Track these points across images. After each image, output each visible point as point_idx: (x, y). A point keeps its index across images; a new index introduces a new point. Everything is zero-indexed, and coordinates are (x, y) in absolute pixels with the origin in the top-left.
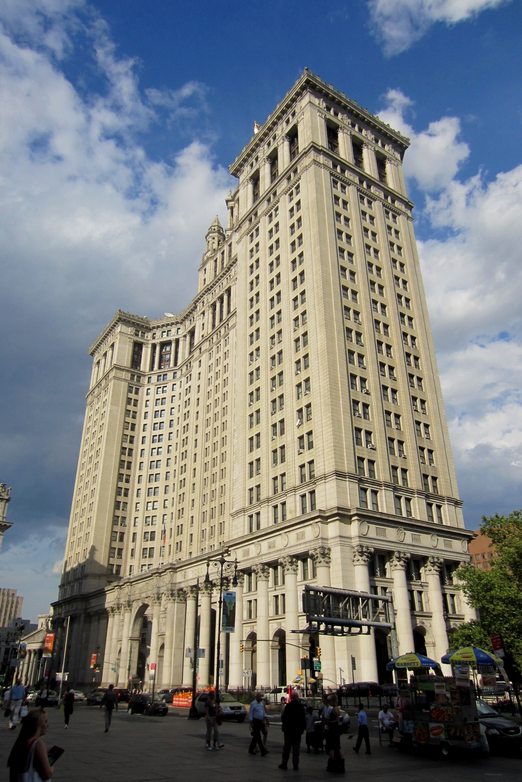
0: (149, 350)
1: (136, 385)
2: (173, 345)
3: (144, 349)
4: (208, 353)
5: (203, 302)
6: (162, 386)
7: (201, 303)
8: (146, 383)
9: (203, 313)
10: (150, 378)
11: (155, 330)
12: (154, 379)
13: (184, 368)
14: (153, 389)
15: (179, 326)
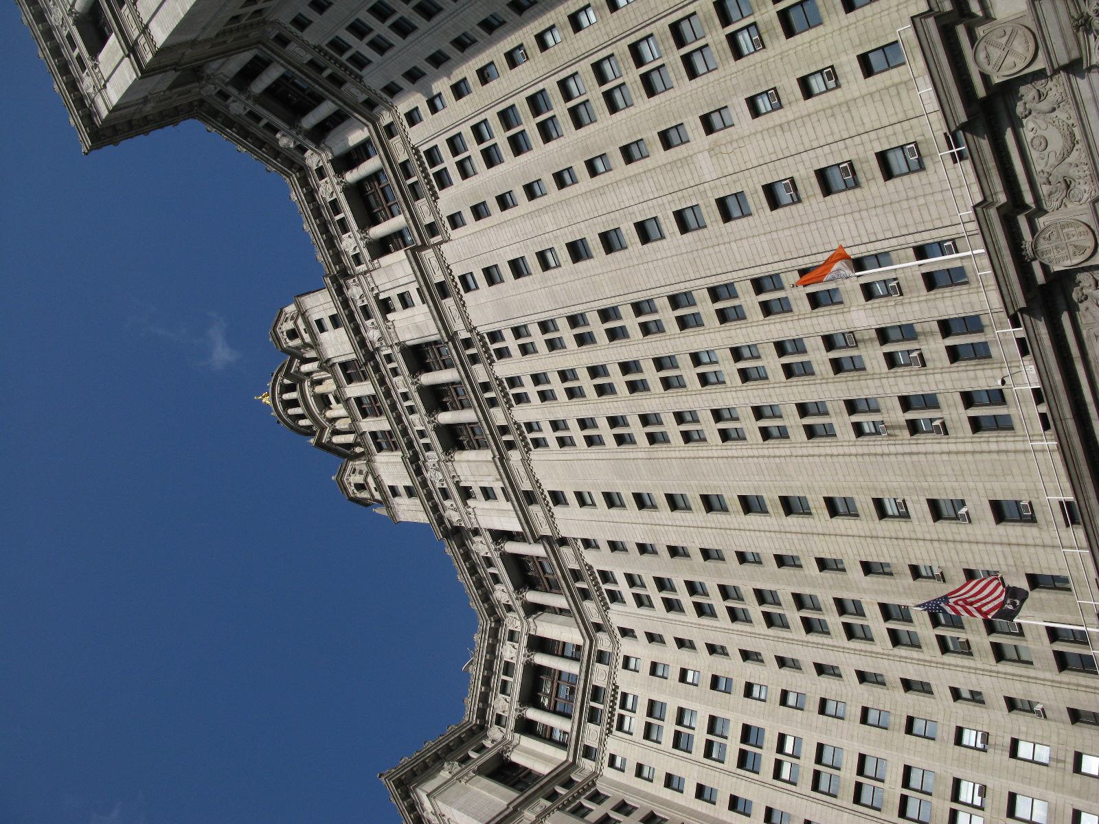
0: (527, 742)
1: (580, 794)
2: (541, 659)
3: (516, 757)
4: (536, 455)
5: (445, 494)
6: (618, 711)
7: (447, 503)
8: (593, 764)
9: (466, 493)
10: (588, 753)
11: (490, 717)
12: (592, 735)
13: (591, 609)
14: (614, 744)
15: (503, 634)
